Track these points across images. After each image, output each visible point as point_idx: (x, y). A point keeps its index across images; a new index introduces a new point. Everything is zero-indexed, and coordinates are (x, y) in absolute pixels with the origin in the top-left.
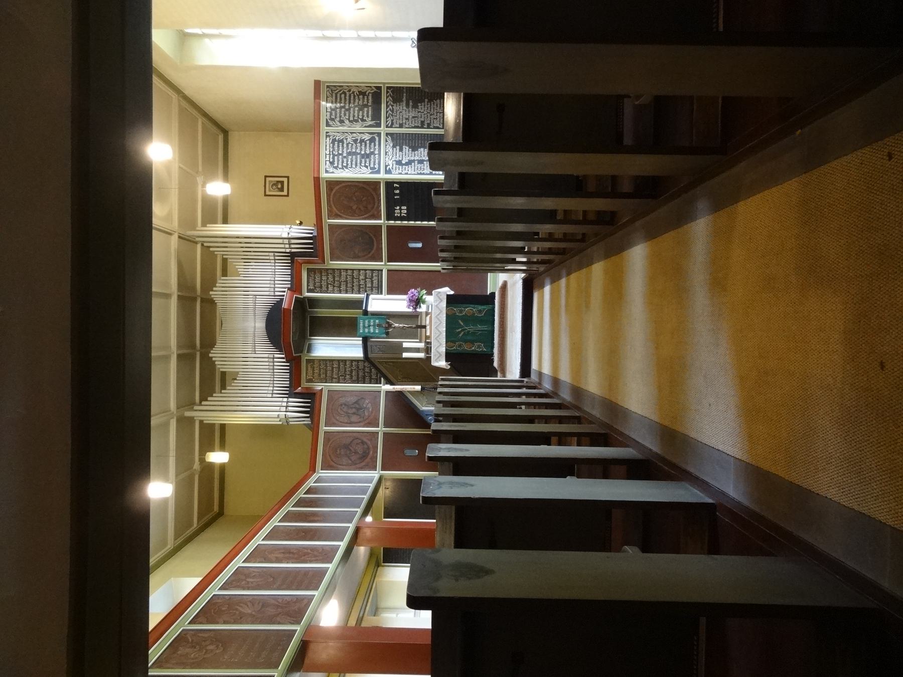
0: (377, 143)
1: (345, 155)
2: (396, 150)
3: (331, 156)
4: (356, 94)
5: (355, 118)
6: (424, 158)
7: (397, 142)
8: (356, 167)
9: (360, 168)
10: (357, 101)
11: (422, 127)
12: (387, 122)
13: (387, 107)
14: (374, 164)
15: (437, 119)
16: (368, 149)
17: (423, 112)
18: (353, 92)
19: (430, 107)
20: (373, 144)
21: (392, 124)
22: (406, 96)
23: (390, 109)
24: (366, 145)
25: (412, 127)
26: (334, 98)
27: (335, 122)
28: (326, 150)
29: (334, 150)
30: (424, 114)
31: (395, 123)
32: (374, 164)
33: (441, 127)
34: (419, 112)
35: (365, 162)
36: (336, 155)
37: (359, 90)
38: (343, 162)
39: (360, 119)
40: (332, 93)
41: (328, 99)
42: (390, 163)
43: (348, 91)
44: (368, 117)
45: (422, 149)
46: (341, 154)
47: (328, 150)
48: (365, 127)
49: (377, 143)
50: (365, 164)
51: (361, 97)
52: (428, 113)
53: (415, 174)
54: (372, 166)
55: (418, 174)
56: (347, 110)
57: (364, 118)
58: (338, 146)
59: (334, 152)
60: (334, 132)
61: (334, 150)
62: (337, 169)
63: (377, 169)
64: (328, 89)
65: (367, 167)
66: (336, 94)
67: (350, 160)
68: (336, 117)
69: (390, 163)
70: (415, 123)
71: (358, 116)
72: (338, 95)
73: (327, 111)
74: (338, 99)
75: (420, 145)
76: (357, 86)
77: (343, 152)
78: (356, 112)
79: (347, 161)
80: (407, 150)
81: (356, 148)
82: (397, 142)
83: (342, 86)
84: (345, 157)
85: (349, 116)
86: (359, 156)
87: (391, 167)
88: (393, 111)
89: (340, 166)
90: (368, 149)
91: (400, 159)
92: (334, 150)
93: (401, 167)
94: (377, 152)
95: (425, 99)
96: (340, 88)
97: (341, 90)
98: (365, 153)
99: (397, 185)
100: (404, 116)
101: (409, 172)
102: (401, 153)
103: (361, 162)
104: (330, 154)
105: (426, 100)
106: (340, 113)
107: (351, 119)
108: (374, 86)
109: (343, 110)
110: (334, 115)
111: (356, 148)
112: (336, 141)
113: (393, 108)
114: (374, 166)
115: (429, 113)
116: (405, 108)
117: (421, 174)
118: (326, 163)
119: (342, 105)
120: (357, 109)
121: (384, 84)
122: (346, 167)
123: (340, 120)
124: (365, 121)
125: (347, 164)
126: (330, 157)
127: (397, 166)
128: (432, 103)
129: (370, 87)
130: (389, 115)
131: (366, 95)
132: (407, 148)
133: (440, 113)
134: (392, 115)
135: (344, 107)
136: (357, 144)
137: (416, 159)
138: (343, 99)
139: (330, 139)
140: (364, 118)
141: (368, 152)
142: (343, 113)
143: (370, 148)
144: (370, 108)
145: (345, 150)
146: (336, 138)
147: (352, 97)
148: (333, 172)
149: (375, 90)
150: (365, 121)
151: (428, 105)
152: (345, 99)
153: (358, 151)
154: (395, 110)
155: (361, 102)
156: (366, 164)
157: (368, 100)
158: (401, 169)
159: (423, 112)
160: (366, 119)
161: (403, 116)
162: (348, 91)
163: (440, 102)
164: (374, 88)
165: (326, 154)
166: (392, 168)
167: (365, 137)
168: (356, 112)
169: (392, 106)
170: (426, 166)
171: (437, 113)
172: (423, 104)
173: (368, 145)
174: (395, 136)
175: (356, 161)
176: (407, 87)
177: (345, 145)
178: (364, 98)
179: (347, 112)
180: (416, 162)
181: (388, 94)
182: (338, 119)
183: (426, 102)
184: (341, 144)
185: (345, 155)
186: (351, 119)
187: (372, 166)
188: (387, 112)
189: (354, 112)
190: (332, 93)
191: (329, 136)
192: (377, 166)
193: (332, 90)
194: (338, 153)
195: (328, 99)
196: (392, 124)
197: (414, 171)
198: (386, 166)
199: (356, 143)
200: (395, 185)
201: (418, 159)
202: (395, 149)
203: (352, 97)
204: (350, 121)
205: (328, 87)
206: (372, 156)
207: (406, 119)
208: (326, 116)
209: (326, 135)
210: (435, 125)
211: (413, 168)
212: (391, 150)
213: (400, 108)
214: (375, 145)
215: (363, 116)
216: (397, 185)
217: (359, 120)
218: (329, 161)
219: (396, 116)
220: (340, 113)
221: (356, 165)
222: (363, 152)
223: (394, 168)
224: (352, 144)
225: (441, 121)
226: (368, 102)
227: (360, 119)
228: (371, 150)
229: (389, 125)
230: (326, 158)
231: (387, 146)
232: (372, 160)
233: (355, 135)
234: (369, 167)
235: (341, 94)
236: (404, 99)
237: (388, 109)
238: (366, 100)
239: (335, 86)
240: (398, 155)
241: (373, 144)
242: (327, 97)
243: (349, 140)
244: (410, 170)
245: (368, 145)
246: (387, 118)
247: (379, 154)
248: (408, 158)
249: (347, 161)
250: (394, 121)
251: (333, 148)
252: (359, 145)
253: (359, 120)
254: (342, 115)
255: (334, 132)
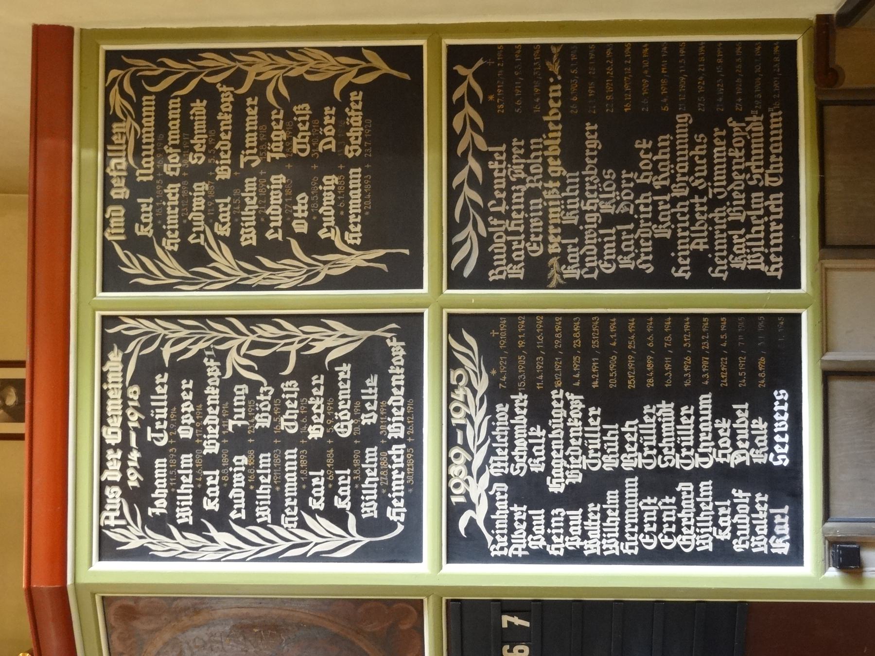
0: (398, 377)
1: (211, 448)
2: (512, 414)
3: (135, 455)
4: (276, 92)
5: (269, 235)
6: (677, 462)
7: (512, 362)
8: (276, 521)
9: (302, 525)
10: (279, 135)
11: (662, 281)
12: (452, 250)
13: (455, 163)
14: (384, 502)
15: (748, 225)
16: (344, 414)
17: (665, 190)
18: (259, 88)
19: (709, 156)
20: (372, 381)
21: (486, 261)
22: (565, 96)
23: (471, 174)
24: (331, 392)
25: (604, 282)
26: (149, 122)
27: (153, 257)
28: (103, 422)
29: (148, 421)
30: (674, 202)
31: (500, 259)
32: (384, 502)
33: (775, 271)
34: (639, 190)
35: (331, 491)
36: (162, 452)
37: (292, 74)
38: (199, 492)
39: (299, 237)
40: (141, 92)
41: (116, 127)
42: (477, 490)
43: (225, 82)
44: (343, 223)
45: (666, 409)
46: (192, 446)
47: (115, 422)
48: (329, 283)
49: (398, 377)
50: (329, 501)
51: (303, 110)
52: (694, 191)
53: (622, 559)
54: (370, 510)
55: (645, 557)
56: (223, 188)
57: (322, 234)
58: (175, 401)
59: (150, 436)
60: (151, 318)
61: (148, 421)
62: (171, 536)
63: (400, 528)
64: (114, 73)
65: (338, 518)
66: (162, 99)
67: (239, 480)
68: (160, 233)
69: (477, 490)
70: (619, 252)
71: (288, 217)
72: (174, 104)
73: (107, 201)
74: (174, 126)
75: (650, 383)
76: (281, 52)
77: (201, 430)
78: (276, 199)
79: (226, 487)
80: (576, 414)
81: (278, 407)
82: (512, 362)
83: (194, 55)
84: (212, 462)
85: (236, 227)
86: (291, 454)
87: (480, 515)
88: (486, 188)
89: (184, 515)
90: (344, 414)
91: (538, 467)
92: (151, 422)
93: (539, 516)
94: (396, 430)
95: (675, 111)
96: (184, 68)
97: (190, 76)
98: (330, 434)
99: (517, 621)
100: (554, 216)
101: (591, 547)
102: (539, 432)
103: (304, 492)
104: (124, 446)
105: (683, 119)
106: (186, 204)
107: (249, 238)
108: (380, 51)
109: (201, 188)
110: (147, 217)
111: (278, 407)
112: (162, 370)
113: (488, 174)
114: (382, 510)
115: (703, 193)
116: (556, 167)
117: (660, 556)
118: (103, 500)
119: (194, 160)
120: (279, 180)
121: (435, 32)
122: (221, 521)
123: (184, 244)
124: (329, 247)
125: (226, 503)
126: (124, 460)
127: (519, 512)
128: (717, 132)
129: (355, 52)
130: (465, 208)
131: (332, 102)
132: (576, 401)
133: (768, 191)
134: (485, 213)
135: (204, 173)
136: (285, 386)
137: (627, 466)
138: (199, 126)
139: (126, 360)
140: (322, 234)
141: (344, 430)
142: (199, 203)
143: (358, 407)
144: (355, 173)
145: (211, 419)
146: (158, 352)
147: (252, 113)
148: (142, 554)
149: (385, 69)
150: (329, 247)
151: (692, 145)
152: (213, 124)
153: (289, 425)
154: (500, 184)
155: (300, 145)
156: (338, 503)
157: (342, 128)
158: (539, 529)
159: (665, 190)
160: (335, 236)
161: (545, 218)
162: (225, 82)
163: (766, 123)
164: (376, 60)
165: (104, 446)
166: (490, 523)
167: (328, 343)
168: (276, 199)
169: (484, 158)
170: (688, 505)
171: (749, 190)
172: (664, 140)
173: (345, 391)
174: (502, 332)
175: (278, 485)
176: (567, 47)
177: (213, 393)
178: (317, 116)
179: (224, 204)
180: (632, 485)
181: (460, 91)
182: (172, 242)
183: (682, 134)
184: (186, 384)
185: (211, 448)
186: (249, 238)
187: (370, 510)
188: (453, 194)
189: (264, 200)
190: (141, 92)
191: (123, 341)
192: (396, 513)
193: (135, 81)
194: (174, 437)
195: (116, 127)
196: (486, 261)
197: (622, 539)
198: (454, 512)
199: (275, 380)
200: (506, 619)
201: (640, 462)
202: (502, 409)
203: (252, 113)
204: (241, 253)
205: (114, 59)
206: (371, 453)
207: (568, 231)
208: (106, 223)
209: (104, 334)
210: (739, 264)
211: (613, 516)
212: (479, 416)
213: (527, 170)
214: (385, 391)
215: (315, 221)
216: (517, 621)
217: (295, 245)
218: (123, 483)
219: (507, 216)
220: (186, 204)
221: (277, 508)
222: (315, 433)
223: (501, 523)
224: (254, 387)
225: (777, 238)
226: (342, 140)
227: (299, 237)
228: (366, 420)
229: (467, 272)
230: (103, 467)
231: (459, 394)
232: (372, 475)
233: (267, 331)
234: (352, 521)
235: (186, 102)
236: (553, 116)
237: (461, 176)
238: (329, 131)
239: (152, 56)
240: (521, 444)
241: (372, 381)
242: (110, 119)
243: (232, 359)
244: (594, 534)
245: (345, 391)
246: (454, 228)
247: (413, 442)
248: (584, 462)
249: (226, 487)
250: (498, 245)
251: (145, 407)
252: (291, 387)
253: (295, 245)
254: (197, 217)
255: (151, 318)
